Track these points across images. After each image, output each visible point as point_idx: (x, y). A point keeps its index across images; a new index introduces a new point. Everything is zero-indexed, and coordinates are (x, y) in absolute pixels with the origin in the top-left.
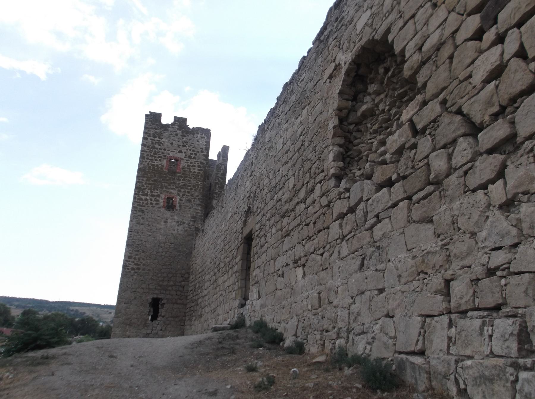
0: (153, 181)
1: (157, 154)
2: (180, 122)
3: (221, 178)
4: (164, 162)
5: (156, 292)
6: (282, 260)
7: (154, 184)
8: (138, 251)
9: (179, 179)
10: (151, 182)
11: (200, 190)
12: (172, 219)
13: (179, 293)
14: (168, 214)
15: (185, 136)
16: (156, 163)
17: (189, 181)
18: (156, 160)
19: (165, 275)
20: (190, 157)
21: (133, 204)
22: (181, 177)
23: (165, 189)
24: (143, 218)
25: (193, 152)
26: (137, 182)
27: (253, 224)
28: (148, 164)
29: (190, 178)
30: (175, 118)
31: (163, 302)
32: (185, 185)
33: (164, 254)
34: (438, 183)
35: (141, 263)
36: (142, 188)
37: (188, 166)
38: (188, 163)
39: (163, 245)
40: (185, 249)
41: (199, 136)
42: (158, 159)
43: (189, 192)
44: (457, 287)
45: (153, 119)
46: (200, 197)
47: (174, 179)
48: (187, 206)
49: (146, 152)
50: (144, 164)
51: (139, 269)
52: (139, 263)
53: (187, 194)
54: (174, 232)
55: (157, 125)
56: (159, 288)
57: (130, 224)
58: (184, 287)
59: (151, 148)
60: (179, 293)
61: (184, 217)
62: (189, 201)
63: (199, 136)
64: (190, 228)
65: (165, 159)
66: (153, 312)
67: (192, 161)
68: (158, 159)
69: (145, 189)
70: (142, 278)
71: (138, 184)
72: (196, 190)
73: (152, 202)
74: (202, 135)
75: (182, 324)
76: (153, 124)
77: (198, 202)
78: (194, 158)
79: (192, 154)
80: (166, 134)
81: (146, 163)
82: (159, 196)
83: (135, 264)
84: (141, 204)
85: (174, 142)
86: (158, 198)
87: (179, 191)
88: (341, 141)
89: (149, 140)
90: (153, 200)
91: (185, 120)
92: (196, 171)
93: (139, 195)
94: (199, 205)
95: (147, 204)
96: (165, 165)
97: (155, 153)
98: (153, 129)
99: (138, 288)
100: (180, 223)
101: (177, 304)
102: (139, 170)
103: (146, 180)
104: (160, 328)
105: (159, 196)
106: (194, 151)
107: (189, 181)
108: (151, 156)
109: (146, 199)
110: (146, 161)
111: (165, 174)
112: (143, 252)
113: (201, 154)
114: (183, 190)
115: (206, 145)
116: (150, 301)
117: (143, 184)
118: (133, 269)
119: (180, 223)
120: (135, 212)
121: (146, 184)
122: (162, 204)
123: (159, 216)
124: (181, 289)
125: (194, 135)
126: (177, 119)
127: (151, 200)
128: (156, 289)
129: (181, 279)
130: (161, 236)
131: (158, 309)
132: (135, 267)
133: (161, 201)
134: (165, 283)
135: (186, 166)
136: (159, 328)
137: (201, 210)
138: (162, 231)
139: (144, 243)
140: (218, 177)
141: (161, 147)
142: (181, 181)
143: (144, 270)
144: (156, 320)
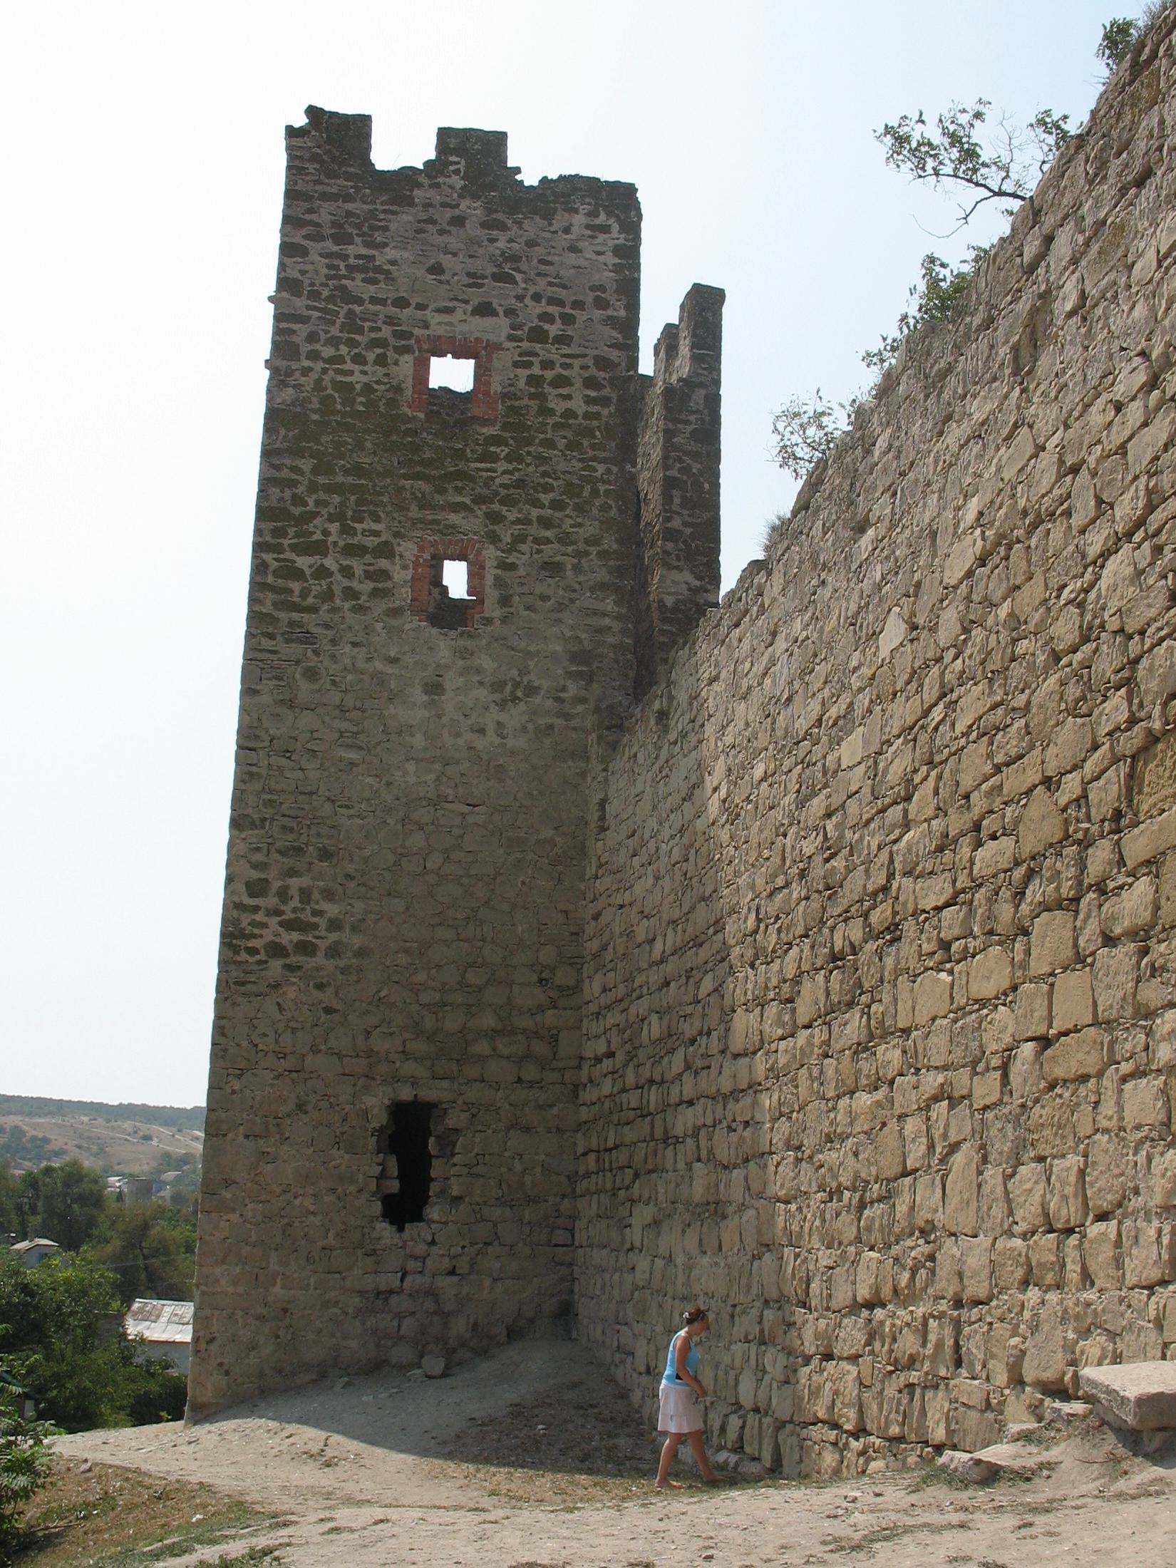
0: (347, 472)
1: (360, 330)
2: (472, 155)
3: (695, 455)
5: (409, 1068)
7: (355, 489)
8: (298, 850)
10: (340, 479)
11: (605, 508)
12: (466, 671)
13: (530, 1072)
15: (503, 227)
16: (358, 379)
18: (359, 359)
21: (253, 600)
22: (497, 440)
23: (414, 512)
24: (311, 674)
25: (551, 309)
26: (266, 483)
28: (319, 386)
29: (550, 444)
30: (445, 135)
31: (451, 1122)
32: (520, 484)
33: (435, 861)
37: (531, 380)
38: (528, 365)
40: (548, 833)
41: (579, 219)
42: (371, 356)
43: (546, 523)
45: (327, 147)
46: (609, 543)
47: (459, 455)
48: (545, 598)
49: (304, 320)
51: (307, 949)
52: (306, 916)
53: (534, 530)
54: (480, 743)
55: (349, 177)
56: (419, 1047)
57: (244, 710)
59: (330, 299)
60: (530, 1072)
62: (553, 568)
63: (579, 219)
64: (568, 717)
65: (407, 350)
66: (401, 1177)
68: (371, 356)
69: (314, 515)
70: (327, 997)
71: (275, 492)
72: (577, 507)
73: (354, 584)
74: (593, 214)
75: (560, 1237)
76: (332, 175)
78: (562, 340)
79: (546, 317)
81: (308, 382)
82: (385, 551)
83: (289, 925)
84: (296, 599)
85: (446, 260)
86: (383, 563)
89: (314, 257)
90: (358, 571)
91: (497, 141)
92: (578, 405)
93: (278, 549)
94: (604, 586)
95: (328, 596)
97: (352, 325)
99: (315, 1050)
100: (510, 692)
101: (528, 1129)
102: (275, 418)
103: (316, 471)
104: (446, 1264)
105: (385, 551)
106: (561, 303)
107: (545, 460)
108: (334, 342)
109: (322, 573)
110: (306, 371)
111: (415, 433)
112: (325, 855)
113: (598, 314)
114: (512, 515)
115: (617, 269)
116: (379, 1117)
117: (301, 489)
118: (276, 950)
119: (510, 692)
120: (266, 643)
121: (313, 488)
122: (406, 594)
123: (394, 661)
124: (539, 1047)
125: (548, 215)
126: (453, 143)
127: (347, 572)
129: (539, 995)
130: (411, 767)
131: (426, 1160)
132: (289, 938)
134: (452, 1023)
135: (522, 384)
136: (438, 1260)
137: (618, 617)
138: (418, 741)
140: (676, 448)
142: (502, 466)
143: (334, 951)
144: (418, 1217)
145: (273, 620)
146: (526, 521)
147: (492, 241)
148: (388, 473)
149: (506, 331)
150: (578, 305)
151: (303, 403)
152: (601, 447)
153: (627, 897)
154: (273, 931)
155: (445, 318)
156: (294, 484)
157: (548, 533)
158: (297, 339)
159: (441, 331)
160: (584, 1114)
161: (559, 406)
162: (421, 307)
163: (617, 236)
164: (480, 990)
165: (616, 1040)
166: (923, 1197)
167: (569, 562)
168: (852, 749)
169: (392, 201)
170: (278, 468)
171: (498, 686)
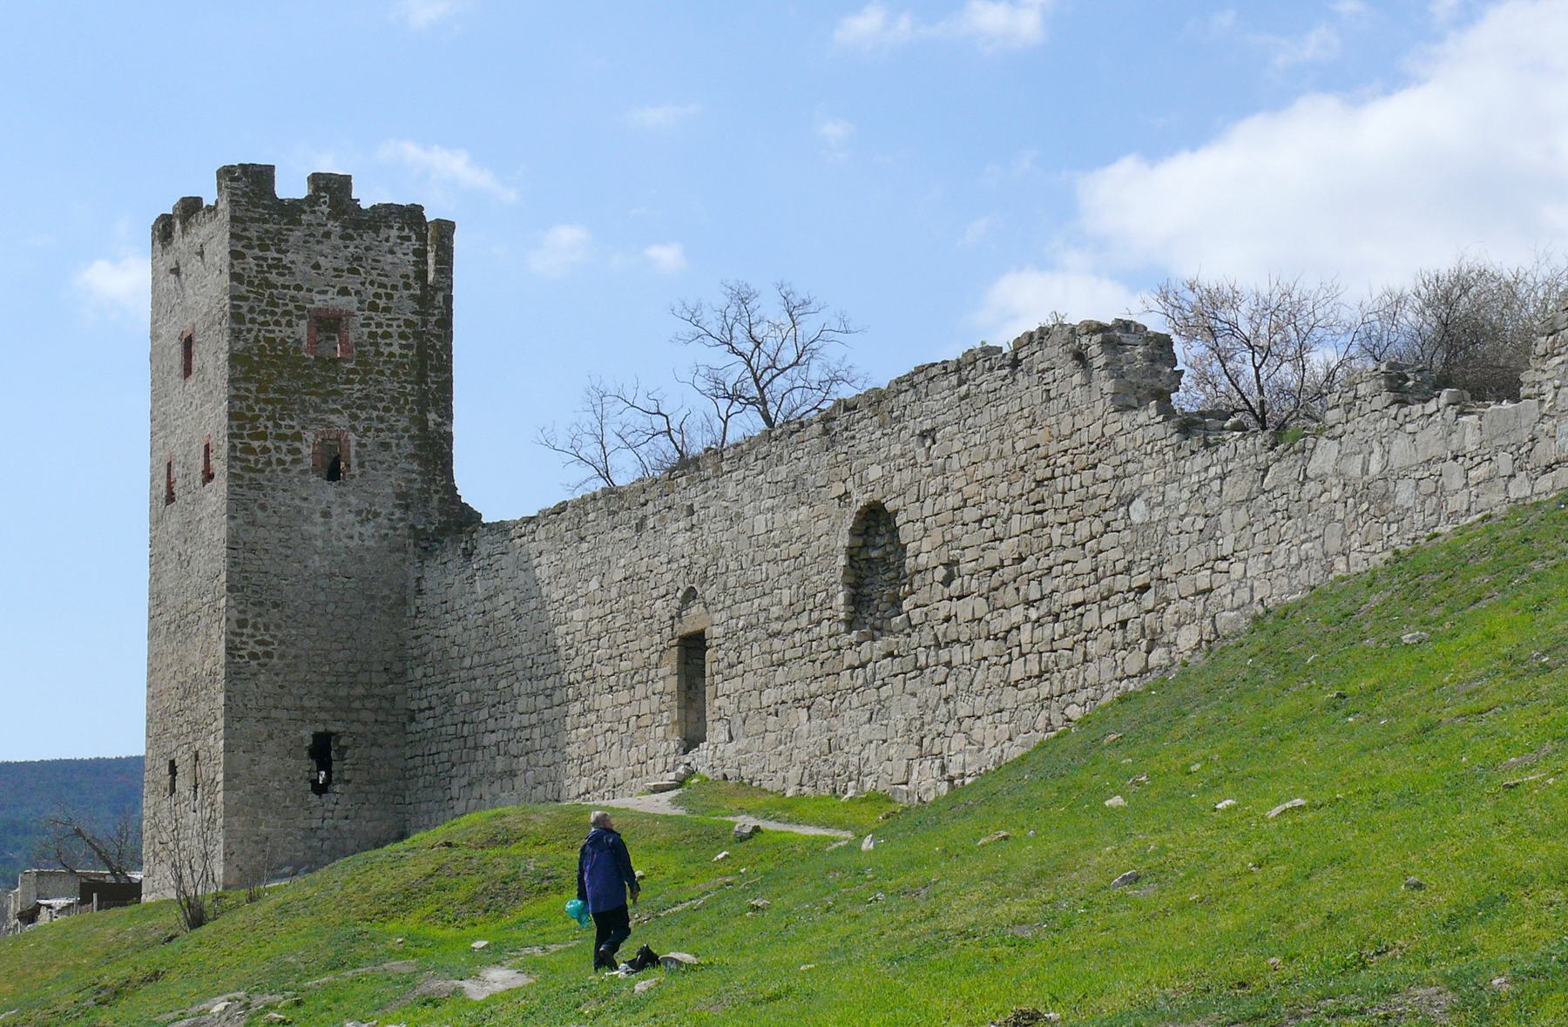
0: (275, 391)
1: (277, 305)
3: (438, 337)
4: (302, 328)
5: (322, 715)
6: (770, 696)
7: (279, 401)
8: (261, 604)
9: (350, 381)
11: (412, 410)
14: (331, 490)
15: (351, 238)
16: (277, 335)
17: (378, 382)
18: (277, 323)
19: (340, 667)
20: (373, 307)
23: (312, 415)
24: (263, 507)
28: (257, 339)
29: (381, 373)
31: (342, 743)
32: (367, 397)
34: (922, 670)
35: (274, 637)
36: (250, 414)
37: (372, 335)
38: (369, 325)
39: (322, 582)
40: (386, 592)
41: (394, 233)
42: (284, 321)
43: (381, 420)
44: (926, 742)
46: (414, 431)
47: (334, 380)
48: (381, 463)
49: (246, 299)
50: (246, 340)
51: (268, 655)
52: (267, 638)
53: (375, 424)
54: (351, 544)
55: (265, 207)
56: (328, 704)
58: (393, 699)
61: (374, 495)
62: (385, 446)
63: (394, 233)
64: (395, 529)
67: (380, 317)
68: (284, 321)
74: (401, 229)
76: (256, 206)
77: (410, 449)
78: (387, 310)
79: (377, 296)
80: (297, 235)
81: (251, 336)
82: (298, 437)
83: (262, 643)
86: (297, 444)
87: (354, 417)
88: (852, 580)
90: (284, 447)
92: (396, 349)
93: (241, 436)
94: (412, 456)
95: (269, 463)
96: (305, 338)
98: (257, 220)
102: (234, 359)
103: (258, 391)
105: (298, 437)
107: (379, 383)
108: (263, 312)
109: (265, 450)
112: (276, 605)
114: (363, 415)
115: (415, 264)
116: (309, 742)
118: (254, 656)
121: (257, 401)
122: (310, 461)
123: (305, 499)
124: (386, 704)
125: (377, 231)
126: (322, 184)
127: (278, 448)
129: (385, 678)
130: (316, 557)
132: (259, 649)
133: (307, 451)
134: (343, 692)
137: (420, 473)
138: (319, 543)
145: (241, 477)
146: (370, 419)
147: (346, 247)
148: (296, 392)
150: (394, 287)
151: (249, 350)
152: (408, 374)
153: (442, 633)
154: (251, 646)
155: (322, 297)
156: (247, 398)
158: (245, 310)
159: (320, 305)
160: (410, 737)
161: (386, 351)
162: (309, 290)
163: (415, 244)
164: (355, 675)
165: (435, 701)
166: (603, 759)
167: (394, 442)
168: (578, 614)
171: (359, 513)
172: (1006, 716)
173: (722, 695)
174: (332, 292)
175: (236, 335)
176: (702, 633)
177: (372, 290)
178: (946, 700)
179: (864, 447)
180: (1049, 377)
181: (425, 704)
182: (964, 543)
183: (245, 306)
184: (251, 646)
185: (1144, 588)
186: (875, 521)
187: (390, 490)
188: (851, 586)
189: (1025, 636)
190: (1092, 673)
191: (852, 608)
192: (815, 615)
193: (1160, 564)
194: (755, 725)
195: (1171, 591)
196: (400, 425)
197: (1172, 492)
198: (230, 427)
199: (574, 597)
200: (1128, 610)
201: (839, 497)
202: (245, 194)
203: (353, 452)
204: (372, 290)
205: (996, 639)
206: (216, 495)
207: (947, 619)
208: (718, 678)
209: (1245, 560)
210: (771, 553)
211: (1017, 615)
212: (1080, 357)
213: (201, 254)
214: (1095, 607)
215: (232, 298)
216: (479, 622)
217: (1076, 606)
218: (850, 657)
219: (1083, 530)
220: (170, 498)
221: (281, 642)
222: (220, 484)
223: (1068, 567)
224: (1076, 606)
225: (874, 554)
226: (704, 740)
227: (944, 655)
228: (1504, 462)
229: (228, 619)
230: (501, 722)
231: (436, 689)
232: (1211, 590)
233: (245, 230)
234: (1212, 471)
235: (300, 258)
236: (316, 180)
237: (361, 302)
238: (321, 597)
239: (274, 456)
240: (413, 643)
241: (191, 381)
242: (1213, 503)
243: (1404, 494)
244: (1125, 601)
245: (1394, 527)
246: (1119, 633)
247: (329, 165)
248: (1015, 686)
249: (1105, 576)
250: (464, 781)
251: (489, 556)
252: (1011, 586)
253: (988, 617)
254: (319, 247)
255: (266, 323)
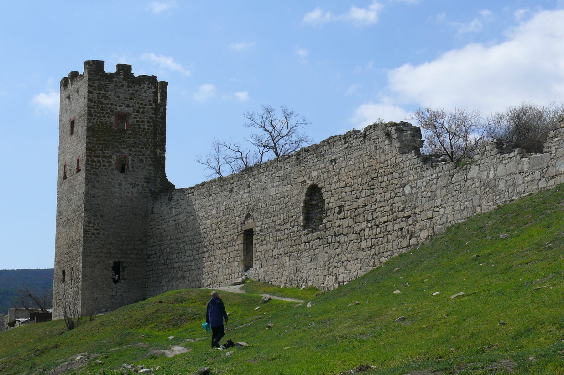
1: (104, 110)
2: (124, 69)
3: (161, 123)
4: (113, 119)
5: (117, 256)
6: (276, 252)
11: (151, 148)
12: (125, 181)
14: (122, 176)
15: (131, 87)
16: (104, 121)
17: (139, 138)
18: (104, 117)
20: (138, 112)
23: (116, 149)
24: (98, 182)
27: (250, 224)
28: (97, 122)
29: (141, 135)
31: (124, 265)
32: (135, 143)
34: (330, 244)
35: (101, 227)
36: (94, 149)
37: (137, 121)
38: (136, 118)
41: (146, 85)
42: (106, 116)
43: (140, 151)
44: (331, 269)
46: (152, 156)
47: (124, 137)
49: (93, 108)
50: (93, 122)
51: (99, 234)
52: (98, 228)
54: (129, 195)
55: (101, 75)
62: (141, 161)
63: (146, 85)
64: (144, 190)
65: (113, 115)
67: (141, 115)
68: (106, 116)
69: (97, 150)
72: (146, 148)
74: (149, 84)
76: (97, 75)
77: (150, 162)
78: (143, 113)
79: (140, 108)
82: (111, 157)
83: (96, 229)
85: (120, 95)
86: (110, 160)
87: (131, 150)
88: (305, 212)
92: (146, 127)
93: (90, 156)
94: (151, 164)
95: (100, 166)
98: (98, 80)
102: (88, 129)
103: (97, 140)
105: (111, 157)
107: (140, 138)
108: (99, 113)
109: (99, 161)
110: (94, 119)
112: (101, 216)
113: (150, 107)
114: (134, 150)
115: (153, 97)
116: (112, 265)
118: (93, 234)
119: (134, 185)
121: (96, 144)
122: (115, 166)
125: (140, 85)
126: (121, 67)
127: (103, 161)
128: (117, 253)
132: (95, 232)
133: (114, 162)
134: (124, 248)
137: (154, 171)
138: (117, 195)
139: (101, 207)
141: (108, 101)
143: (103, 234)
149: (132, 111)
153: (160, 227)
154: (92, 230)
156: (93, 143)
157: (140, 154)
158: (93, 112)
159: (119, 110)
160: (148, 264)
162: (116, 105)
163: (153, 89)
165: (157, 251)
166: (216, 273)
168: (208, 222)
169: (109, 81)
170: (90, 140)
171: (132, 184)
172: (359, 261)
173: (259, 251)
174: (124, 106)
175: (89, 121)
176: (252, 229)
177: (138, 106)
178: (338, 255)
179: (311, 165)
180: (377, 141)
181: (153, 252)
182: (345, 200)
183: (93, 110)
184: (92, 230)
185: (409, 217)
186: (314, 191)
187: (142, 176)
188: (305, 214)
189: (366, 233)
190: (390, 246)
191: (305, 222)
192: (292, 224)
193: (415, 208)
194: (270, 262)
195: (418, 218)
196: (147, 153)
197: (419, 183)
198: (87, 153)
199: (207, 215)
200: (403, 224)
201: (302, 182)
202: (93, 71)
203: (130, 163)
204: (138, 106)
205: (356, 233)
206: (81, 177)
207: (339, 226)
208: (257, 245)
209: (445, 207)
210: (277, 201)
211: (364, 225)
212: (388, 135)
213: (78, 92)
214: (391, 223)
215: (88, 107)
216: (173, 224)
217: (385, 222)
218: (304, 239)
219: (388, 196)
220: (65, 177)
221: (103, 229)
222: (83, 173)
223: (382, 209)
224: (385, 222)
225: (314, 203)
226: (252, 267)
227: (338, 239)
228: (537, 175)
229: (84, 221)
230: (180, 259)
231: (158, 247)
232: (432, 218)
233: (93, 83)
234: (434, 176)
235: (113, 94)
236: (119, 66)
237: (134, 110)
238: (118, 214)
239: (102, 163)
240: (150, 231)
241: (73, 136)
242: (434, 187)
243: (502, 185)
244: (402, 221)
245: (498, 197)
246: (400, 232)
247: (123, 61)
248: (363, 250)
249: (395, 212)
250: (167, 280)
251: (177, 200)
252: (362, 215)
253: (353, 226)
254: (119, 90)
255: (100, 117)
